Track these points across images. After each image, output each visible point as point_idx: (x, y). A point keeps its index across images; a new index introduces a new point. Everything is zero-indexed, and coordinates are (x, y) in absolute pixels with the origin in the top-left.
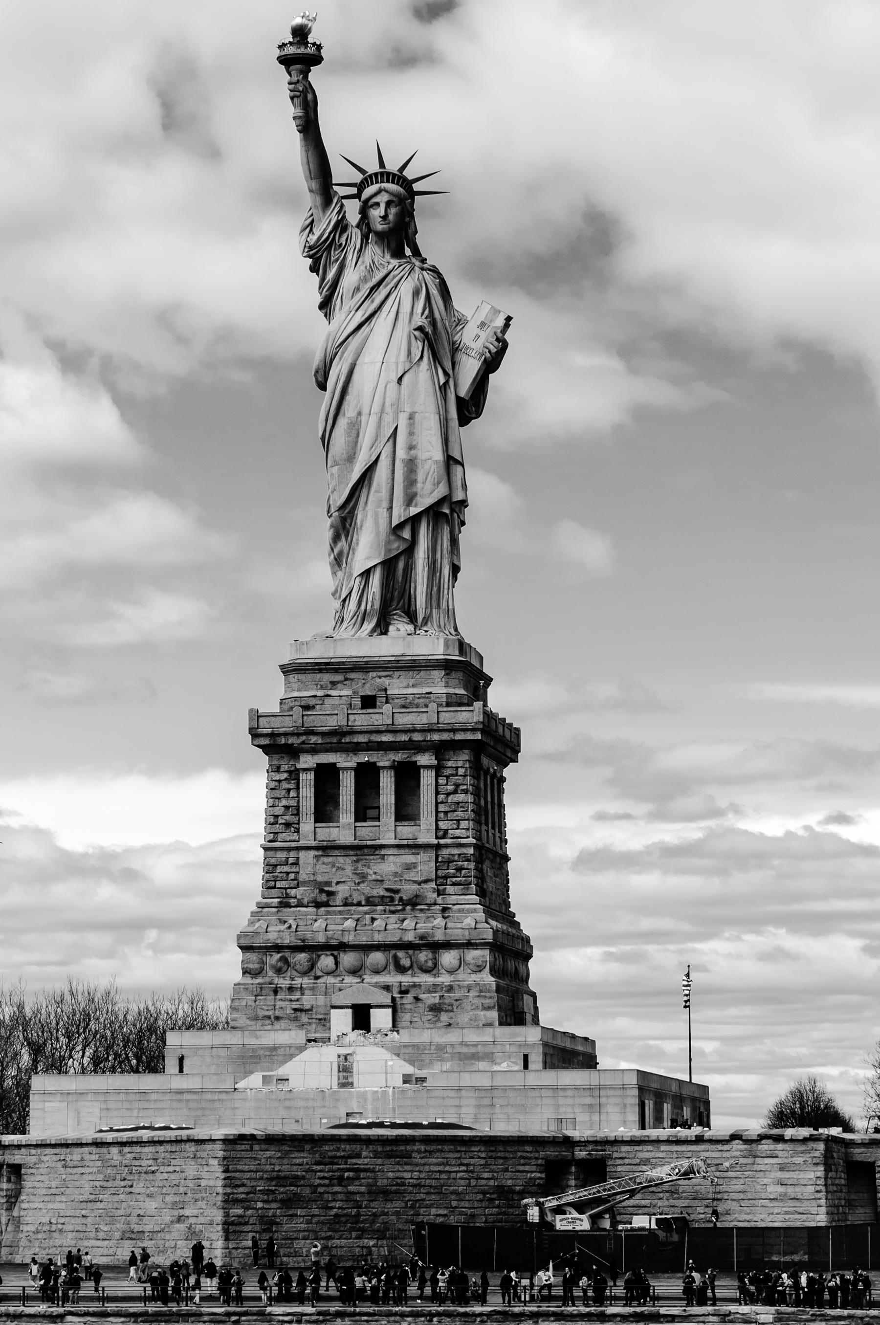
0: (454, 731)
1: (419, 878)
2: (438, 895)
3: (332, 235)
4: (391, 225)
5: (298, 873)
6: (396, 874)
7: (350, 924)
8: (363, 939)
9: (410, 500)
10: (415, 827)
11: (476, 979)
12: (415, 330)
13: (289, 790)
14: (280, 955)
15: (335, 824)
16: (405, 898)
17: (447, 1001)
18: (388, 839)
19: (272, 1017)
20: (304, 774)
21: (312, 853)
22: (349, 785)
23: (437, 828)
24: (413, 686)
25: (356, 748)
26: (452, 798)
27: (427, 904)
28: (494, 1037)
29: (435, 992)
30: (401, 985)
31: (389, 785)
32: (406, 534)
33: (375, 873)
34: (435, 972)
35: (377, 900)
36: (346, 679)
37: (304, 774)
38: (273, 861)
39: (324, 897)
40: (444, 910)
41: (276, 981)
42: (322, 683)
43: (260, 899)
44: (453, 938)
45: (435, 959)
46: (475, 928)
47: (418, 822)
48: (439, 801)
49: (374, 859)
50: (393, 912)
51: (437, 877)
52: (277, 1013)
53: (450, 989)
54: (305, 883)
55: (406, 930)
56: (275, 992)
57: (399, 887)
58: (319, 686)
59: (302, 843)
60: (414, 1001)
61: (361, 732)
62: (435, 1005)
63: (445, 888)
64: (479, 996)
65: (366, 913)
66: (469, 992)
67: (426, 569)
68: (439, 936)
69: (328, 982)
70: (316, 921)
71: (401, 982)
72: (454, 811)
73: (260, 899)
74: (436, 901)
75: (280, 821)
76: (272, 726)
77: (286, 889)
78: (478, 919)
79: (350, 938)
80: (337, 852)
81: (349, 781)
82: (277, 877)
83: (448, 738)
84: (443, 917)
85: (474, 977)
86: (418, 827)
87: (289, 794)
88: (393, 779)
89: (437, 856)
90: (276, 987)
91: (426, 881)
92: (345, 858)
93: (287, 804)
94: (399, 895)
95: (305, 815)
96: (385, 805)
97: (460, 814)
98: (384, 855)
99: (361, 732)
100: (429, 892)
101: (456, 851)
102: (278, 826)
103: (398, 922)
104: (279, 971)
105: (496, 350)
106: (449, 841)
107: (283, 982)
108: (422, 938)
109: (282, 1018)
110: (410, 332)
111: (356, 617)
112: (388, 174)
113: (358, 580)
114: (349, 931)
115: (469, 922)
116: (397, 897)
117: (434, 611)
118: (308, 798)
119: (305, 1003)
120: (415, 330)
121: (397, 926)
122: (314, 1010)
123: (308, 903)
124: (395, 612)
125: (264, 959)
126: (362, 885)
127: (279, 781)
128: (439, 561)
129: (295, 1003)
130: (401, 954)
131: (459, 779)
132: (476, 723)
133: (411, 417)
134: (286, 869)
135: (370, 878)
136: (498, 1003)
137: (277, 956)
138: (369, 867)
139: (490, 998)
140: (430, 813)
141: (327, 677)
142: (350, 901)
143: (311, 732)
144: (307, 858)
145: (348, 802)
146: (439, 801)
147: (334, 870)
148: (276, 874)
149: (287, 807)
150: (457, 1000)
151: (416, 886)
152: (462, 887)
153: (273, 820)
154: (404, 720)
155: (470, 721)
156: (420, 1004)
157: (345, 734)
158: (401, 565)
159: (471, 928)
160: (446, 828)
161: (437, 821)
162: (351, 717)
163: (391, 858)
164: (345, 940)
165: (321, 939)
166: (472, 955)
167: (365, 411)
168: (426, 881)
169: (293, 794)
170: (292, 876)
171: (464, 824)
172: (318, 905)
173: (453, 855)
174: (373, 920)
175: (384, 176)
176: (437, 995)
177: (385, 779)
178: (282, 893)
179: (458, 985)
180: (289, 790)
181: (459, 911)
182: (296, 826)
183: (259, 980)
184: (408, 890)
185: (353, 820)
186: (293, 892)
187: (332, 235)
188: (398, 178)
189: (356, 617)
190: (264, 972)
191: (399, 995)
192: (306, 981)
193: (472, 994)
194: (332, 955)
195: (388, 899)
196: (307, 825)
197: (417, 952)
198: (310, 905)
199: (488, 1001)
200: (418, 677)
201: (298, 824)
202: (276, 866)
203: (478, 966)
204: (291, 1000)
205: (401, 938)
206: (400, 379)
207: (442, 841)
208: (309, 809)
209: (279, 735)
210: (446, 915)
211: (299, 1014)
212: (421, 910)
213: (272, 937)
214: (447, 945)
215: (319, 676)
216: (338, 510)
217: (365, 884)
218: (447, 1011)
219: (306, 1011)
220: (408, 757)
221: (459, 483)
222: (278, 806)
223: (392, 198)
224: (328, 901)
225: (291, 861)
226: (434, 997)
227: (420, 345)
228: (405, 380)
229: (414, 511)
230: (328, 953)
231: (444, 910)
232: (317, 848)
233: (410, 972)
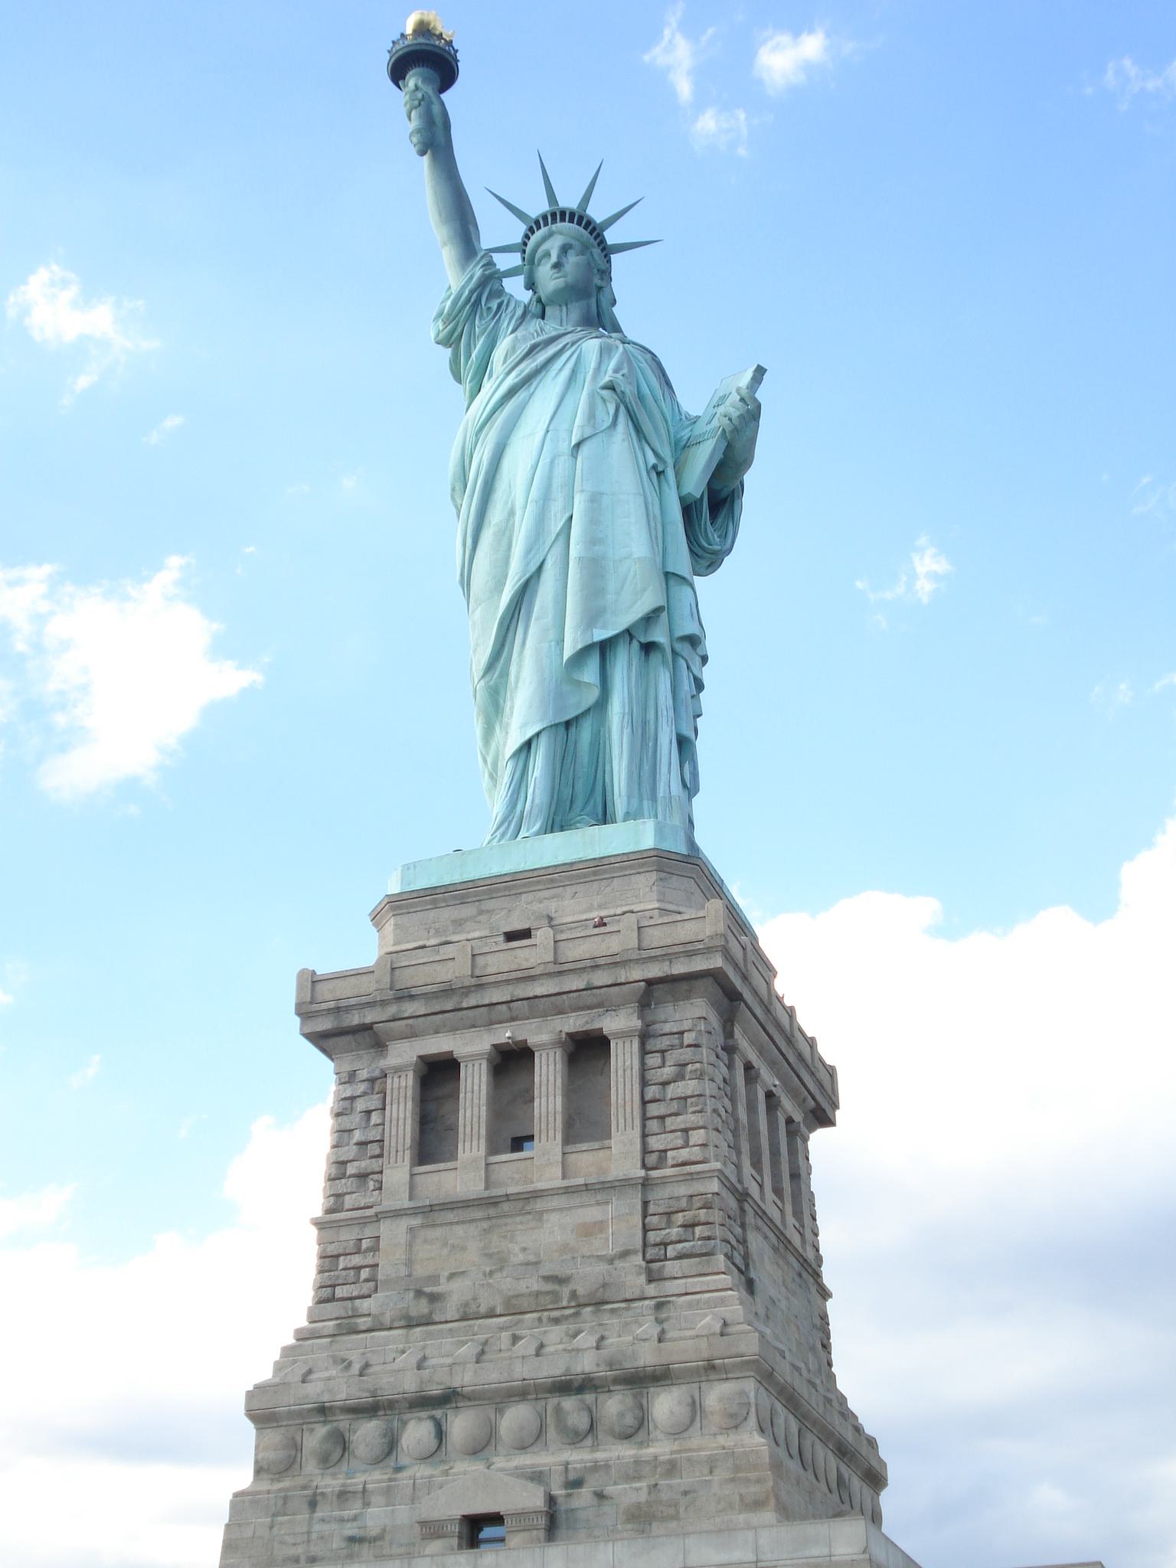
0: (669, 957)
1: (610, 1251)
2: (650, 1281)
3: (475, 295)
4: (570, 279)
5: (377, 1265)
6: (565, 1248)
7: (468, 1350)
8: (491, 1376)
9: (592, 616)
10: (601, 1153)
11: (727, 1444)
12: (605, 388)
13: (369, 1112)
14: (328, 1427)
15: (449, 1165)
16: (581, 1291)
17: (664, 1496)
18: (551, 1177)
19: (303, 1559)
20: (396, 1080)
21: (404, 1223)
22: (476, 1088)
23: (645, 1151)
24: (600, 907)
25: (492, 1014)
26: (673, 1090)
27: (626, 1301)
28: (756, 1550)
29: (639, 1478)
30: (566, 1469)
31: (551, 1079)
32: (590, 673)
33: (524, 1249)
34: (641, 1435)
35: (525, 1304)
36: (481, 912)
37: (396, 1080)
38: (332, 1249)
39: (422, 1307)
40: (659, 1306)
41: (317, 1481)
42: (437, 925)
43: (303, 1323)
44: (675, 1358)
45: (641, 1407)
46: (722, 1335)
47: (606, 1143)
48: (649, 1096)
49: (521, 1223)
50: (556, 1321)
51: (645, 1245)
52: (315, 1550)
53: (672, 1468)
54: (388, 1282)
55: (578, 1350)
56: (313, 1504)
57: (569, 1272)
58: (432, 931)
59: (388, 1204)
60: (595, 1501)
61: (497, 984)
62: (638, 1506)
63: (664, 1266)
64: (732, 1480)
65: (502, 1329)
66: (711, 1472)
67: (627, 731)
68: (647, 1357)
69: (418, 1475)
70: (403, 1352)
71: (567, 1463)
72: (676, 1114)
73: (303, 1323)
74: (643, 1292)
75: (351, 1169)
76: (338, 995)
77: (351, 1299)
78: (729, 1319)
79: (466, 1379)
80: (450, 1216)
81: (476, 1081)
82: (338, 1277)
83: (660, 974)
84: (659, 1321)
85: (722, 1440)
86: (607, 1151)
87: (368, 1119)
88: (559, 1066)
89: (645, 1204)
90: (315, 1495)
91: (625, 1254)
92: (466, 1226)
93: (363, 1139)
94: (572, 1286)
95: (393, 1154)
96: (544, 1114)
97: (689, 1119)
98: (541, 1213)
99: (497, 984)
100: (631, 1277)
101: (683, 1190)
102: (343, 1181)
103: (566, 1339)
104: (325, 1461)
105: (738, 413)
106: (668, 1172)
107: (330, 1483)
108: (611, 1365)
109: (323, 1559)
110: (593, 391)
111: (506, 824)
112: (563, 213)
113: (510, 766)
114: (464, 1363)
115: (708, 1322)
116: (565, 1292)
117: (645, 803)
118: (401, 1122)
119: (370, 1523)
120: (605, 388)
121: (561, 1347)
122: (388, 1537)
123: (392, 1321)
124: (578, 818)
125: (298, 1439)
126: (497, 1275)
127: (352, 1099)
128: (652, 723)
129: (349, 1525)
130: (569, 1403)
131: (687, 1054)
132: (711, 937)
133: (595, 499)
134: (357, 1260)
135: (514, 1260)
136: (773, 1491)
137: (322, 1431)
138: (511, 1241)
139: (758, 1481)
140: (629, 1120)
141: (446, 914)
142: (473, 1308)
143: (405, 996)
144: (393, 1233)
145: (475, 1119)
146: (648, 1097)
147: (445, 1251)
148: (336, 1273)
149: (362, 1144)
150: (685, 1493)
151: (603, 1267)
152: (698, 1259)
153: (338, 1170)
154: (576, 951)
155: (700, 938)
156: (608, 1508)
157: (467, 990)
158: (585, 733)
159: (714, 1334)
160: (661, 1148)
161: (644, 1136)
162: (480, 961)
163: (554, 1218)
164: (456, 1383)
165: (410, 1384)
166: (716, 1395)
167: (519, 504)
168: (625, 1254)
169: (375, 1118)
170: (365, 1274)
171: (697, 1137)
172: (411, 1323)
173: (678, 1198)
174: (515, 1339)
175: (559, 215)
176: (643, 1484)
177: (544, 1068)
178: (345, 1308)
179: (689, 1460)
180: (369, 1112)
181: (690, 1305)
182: (375, 1177)
183: (286, 1484)
184: (587, 1276)
185: (483, 1152)
186: (364, 1305)
187: (475, 295)
188: (578, 217)
189: (506, 824)
190: (297, 1466)
191: (563, 1492)
192: (376, 1478)
193: (721, 1474)
194: (432, 1418)
195: (548, 1298)
196: (397, 1173)
197: (602, 1397)
198: (396, 1324)
199: (753, 1489)
200: (608, 889)
201: (381, 1172)
202: (338, 1256)
203: (732, 1416)
204: (342, 1520)
205: (568, 1369)
206: (578, 445)
207: (654, 1174)
208: (401, 1141)
209: (348, 1009)
210: (664, 1316)
211: (356, 1547)
212: (613, 1311)
213: (314, 1391)
214: (661, 1377)
215: (432, 913)
216: (483, 676)
217: (504, 1273)
218: (664, 1519)
219: (375, 1539)
220: (587, 1023)
221: (687, 611)
222: (348, 1144)
223: (569, 240)
224: (431, 1313)
225: (365, 1244)
226: (637, 1489)
227: (612, 409)
228: (585, 449)
229: (600, 635)
230: (424, 1414)
231: (659, 1306)
232: (414, 1212)
233: (588, 1442)
